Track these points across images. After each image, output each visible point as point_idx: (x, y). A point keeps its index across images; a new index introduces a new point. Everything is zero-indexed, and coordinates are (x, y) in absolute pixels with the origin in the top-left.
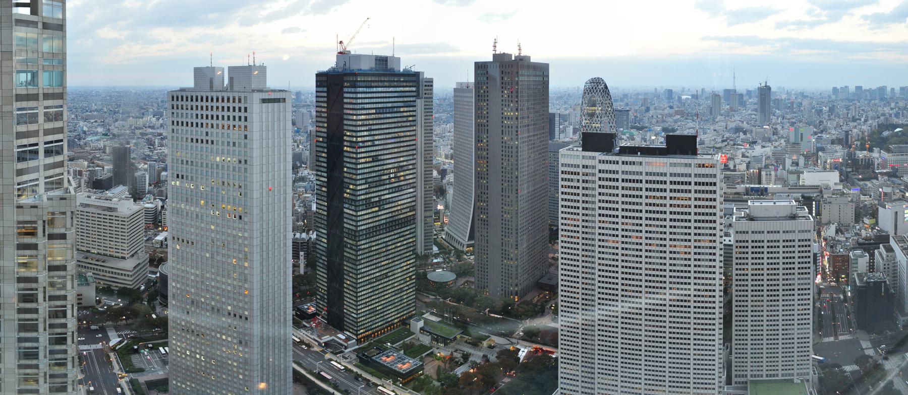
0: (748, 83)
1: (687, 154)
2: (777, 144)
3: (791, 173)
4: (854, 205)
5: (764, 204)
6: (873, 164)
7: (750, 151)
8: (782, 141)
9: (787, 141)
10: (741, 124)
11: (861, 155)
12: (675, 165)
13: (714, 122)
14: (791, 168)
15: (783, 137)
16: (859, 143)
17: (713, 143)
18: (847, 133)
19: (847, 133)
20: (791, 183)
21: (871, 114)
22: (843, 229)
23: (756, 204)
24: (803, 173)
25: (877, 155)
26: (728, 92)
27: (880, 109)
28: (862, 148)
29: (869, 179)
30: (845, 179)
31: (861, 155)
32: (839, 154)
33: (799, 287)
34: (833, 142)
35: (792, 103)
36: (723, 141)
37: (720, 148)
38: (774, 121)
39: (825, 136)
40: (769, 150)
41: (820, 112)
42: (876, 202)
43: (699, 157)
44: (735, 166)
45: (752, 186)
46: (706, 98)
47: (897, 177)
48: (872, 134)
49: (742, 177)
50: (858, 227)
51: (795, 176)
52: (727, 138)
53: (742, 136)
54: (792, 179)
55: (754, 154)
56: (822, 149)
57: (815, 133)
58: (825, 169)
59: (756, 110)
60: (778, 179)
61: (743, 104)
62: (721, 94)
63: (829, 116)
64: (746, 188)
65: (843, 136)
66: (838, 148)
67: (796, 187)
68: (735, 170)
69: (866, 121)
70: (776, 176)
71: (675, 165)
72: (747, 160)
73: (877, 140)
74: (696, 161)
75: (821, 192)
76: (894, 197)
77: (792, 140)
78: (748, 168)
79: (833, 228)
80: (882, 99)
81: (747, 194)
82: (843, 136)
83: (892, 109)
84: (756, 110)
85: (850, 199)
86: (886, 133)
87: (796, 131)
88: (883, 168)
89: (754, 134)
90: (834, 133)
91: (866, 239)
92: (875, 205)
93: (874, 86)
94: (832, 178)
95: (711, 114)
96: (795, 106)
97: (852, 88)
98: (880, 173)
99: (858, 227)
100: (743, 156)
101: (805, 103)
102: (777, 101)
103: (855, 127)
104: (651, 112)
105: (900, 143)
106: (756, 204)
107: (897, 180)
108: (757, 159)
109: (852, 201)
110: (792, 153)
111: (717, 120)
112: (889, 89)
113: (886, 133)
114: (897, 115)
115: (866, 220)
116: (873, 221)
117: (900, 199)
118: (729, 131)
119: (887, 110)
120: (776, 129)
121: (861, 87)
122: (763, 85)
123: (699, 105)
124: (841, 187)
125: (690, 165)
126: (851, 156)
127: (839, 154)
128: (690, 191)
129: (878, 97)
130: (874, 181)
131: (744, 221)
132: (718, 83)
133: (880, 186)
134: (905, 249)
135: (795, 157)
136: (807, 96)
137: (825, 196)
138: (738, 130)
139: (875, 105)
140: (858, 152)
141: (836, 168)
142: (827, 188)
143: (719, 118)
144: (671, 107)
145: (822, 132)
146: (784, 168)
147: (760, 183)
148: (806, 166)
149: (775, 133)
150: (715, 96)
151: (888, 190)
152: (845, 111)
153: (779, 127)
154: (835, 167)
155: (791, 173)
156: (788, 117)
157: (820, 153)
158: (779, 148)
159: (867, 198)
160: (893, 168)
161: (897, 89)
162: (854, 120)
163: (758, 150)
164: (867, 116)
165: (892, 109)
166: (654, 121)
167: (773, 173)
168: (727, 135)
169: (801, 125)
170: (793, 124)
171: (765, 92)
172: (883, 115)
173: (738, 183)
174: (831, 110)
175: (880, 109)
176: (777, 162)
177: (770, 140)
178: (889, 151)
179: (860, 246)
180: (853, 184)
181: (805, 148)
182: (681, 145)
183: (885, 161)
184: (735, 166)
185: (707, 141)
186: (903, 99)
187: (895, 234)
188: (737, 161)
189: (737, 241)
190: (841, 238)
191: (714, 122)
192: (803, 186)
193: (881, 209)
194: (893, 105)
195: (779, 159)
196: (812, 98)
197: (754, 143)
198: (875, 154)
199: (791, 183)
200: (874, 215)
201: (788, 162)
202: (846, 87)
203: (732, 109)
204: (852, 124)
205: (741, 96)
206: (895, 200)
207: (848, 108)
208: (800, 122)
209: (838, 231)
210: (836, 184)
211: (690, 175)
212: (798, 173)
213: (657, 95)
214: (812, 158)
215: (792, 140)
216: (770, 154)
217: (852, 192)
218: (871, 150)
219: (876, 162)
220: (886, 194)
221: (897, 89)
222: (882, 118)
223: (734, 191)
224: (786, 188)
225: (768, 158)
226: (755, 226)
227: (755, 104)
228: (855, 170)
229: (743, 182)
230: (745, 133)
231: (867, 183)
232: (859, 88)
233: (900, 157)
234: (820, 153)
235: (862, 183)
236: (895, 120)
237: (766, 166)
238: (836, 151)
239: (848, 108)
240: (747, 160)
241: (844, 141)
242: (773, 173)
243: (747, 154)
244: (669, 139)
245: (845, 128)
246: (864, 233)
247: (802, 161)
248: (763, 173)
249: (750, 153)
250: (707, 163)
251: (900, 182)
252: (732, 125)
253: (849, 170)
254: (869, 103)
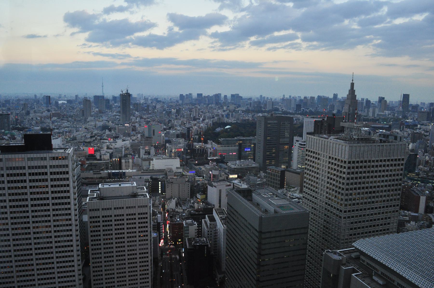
0: (112, 91)
1: (44, 150)
2: (135, 138)
3: (145, 160)
4: (190, 184)
5: (112, 186)
6: (206, 152)
7: (113, 144)
8: (139, 136)
9: (143, 136)
10: (107, 123)
11: (197, 145)
12: (32, 159)
13: (86, 121)
14: (144, 156)
15: (139, 133)
16: (197, 137)
17: (83, 138)
18: (189, 129)
19: (189, 129)
20: (145, 168)
21: (207, 114)
22: (181, 203)
23: (105, 186)
24: (152, 160)
25: (210, 146)
26: (97, 98)
27: (215, 111)
28: (200, 141)
29: (203, 164)
30: (185, 164)
31: (197, 145)
32: (181, 145)
33: (140, 252)
34: (178, 136)
35: (148, 106)
36: (91, 137)
37: (89, 142)
38: (133, 120)
39: (172, 131)
40: (128, 143)
41: (169, 113)
42: (206, 182)
43: (54, 151)
44: (101, 156)
45: (113, 171)
46: (80, 103)
47: (223, 162)
48: (208, 129)
49: (107, 164)
50: (192, 201)
51: (147, 163)
52: (96, 134)
53: (107, 132)
54: (145, 164)
55: (116, 146)
56: (169, 142)
57: (165, 129)
58: (170, 157)
59: (119, 112)
60: (135, 165)
61: (109, 107)
62: (92, 100)
63: (176, 116)
64: (109, 173)
65: (185, 132)
66: (182, 140)
67: (148, 171)
68: (100, 160)
69: (204, 120)
70: (133, 162)
71: (32, 159)
72: (111, 151)
73: (210, 135)
74: (50, 155)
75: (166, 174)
76: (221, 178)
77: (146, 134)
78: (111, 156)
79: (174, 202)
80: (217, 103)
81: (110, 178)
82: (185, 132)
83: (224, 111)
84: (119, 112)
85: (187, 179)
86: (218, 130)
87: (149, 127)
88: (214, 156)
89: (117, 131)
90: (179, 129)
91: (198, 210)
92: (206, 184)
93: (211, 93)
94: (175, 164)
95: (83, 115)
96: (150, 109)
97: (195, 96)
98: (211, 160)
99: (192, 201)
100: (108, 148)
101: (158, 106)
102: (137, 106)
103: (195, 125)
104: (32, 115)
105: (229, 137)
106: (105, 186)
107: (224, 165)
108: (118, 150)
109: (188, 181)
110: (146, 145)
111: (88, 120)
112: (223, 96)
113: (218, 130)
114: (228, 116)
115: (199, 196)
116: (204, 196)
117: (224, 180)
118: (97, 129)
119: (220, 112)
120: (134, 126)
121: (201, 95)
122: (124, 92)
123: (73, 108)
124: (181, 170)
125: (45, 159)
126: (190, 147)
127: (181, 145)
128: (47, 180)
129: (214, 102)
130: (207, 166)
131: (96, 201)
132: (90, 91)
133: (209, 169)
134: (223, 219)
135: (147, 148)
136: (160, 101)
137: (169, 178)
138: (105, 128)
139: (212, 108)
140: (195, 143)
141: (179, 156)
142: (171, 171)
143: (89, 118)
144: (48, 111)
145: (170, 128)
146: (139, 156)
147: (120, 169)
148: (156, 154)
149: (134, 129)
150: (86, 101)
151: (216, 173)
152: (189, 113)
153: (137, 125)
154: (179, 155)
155: (145, 160)
156: (145, 117)
157: (167, 145)
158: (136, 141)
159: (201, 178)
160: (221, 156)
161: (229, 96)
162: (195, 119)
163: (120, 143)
164: (204, 117)
165: (224, 111)
166: (34, 122)
167: (131, 161)
168: (95, 132)
169: (153, 123)
170: (148, 123)
171: (126, 98)
172: (217, 115)
173: (102, 170)
174: (178, 112)
175: (215, 111)
176: (134, 152)
177: (129, 135)
178: (218, 143)
179: (192, 216)
180: (191, 169)
181: (156, 141)
182: (39, 142)
183: (215, 150)
184: (101, 156)
185: (78, 137)
186: (233, 104)
187: (220, 206)
188: (103, 152)
189: (91, 218)
190: (180, 210)
191: (86, 121)
192: (153, 170)
193: (209, 187)
194: (225, 108)
195: (135, 149)
196: (164, 103)
197: (117, 137)
198: (209, 146)
199: (145, 168)
200: (204, 192)
201: (142, 152)
202: (190, 94)
203: (100, 112)
204: (193, 122)
205: (108, 101)
206: (220, 181)
207: (191, 110)
208: (154, 121)
209: (178, 204)
210: (177, 168)
211: (46, 167)
212: (150, 160)
213: (37, 101)
214: (161, 149)
215: (146, 134)
216: (129, 146)
217: (189, 174)
218: (206, 142)
219: (209, 151)
220: (214, 176)
221: (229, 96)
222: (216, 118)
223: (99, 176)
224: (140, 172)
225: (127, 149)
226: (106, 204)
227: (119, 107)
228: (193, 157)
229: (107, 169)
230: (110, 130)
231: (201, 167)
232: (199, 95)
233: (227, 148)
234: (167, 145)
235: (198, 167)
236: (226, 120)
237: (126, 156)
238: (180, 143)
239: (191, 110)
240: (111, 151)
241: (186, 135)
242: (131, 161)
243: (111, 147)
244: (26, 137)
245: (187, 125)
246: (196, 205)
247: (153, 151)
248: (123, 161)
249: (114, 145)
250: (60, 156)
251: (226, 167)
252: (100, 124)
253: (188, 157)
254: (207, 107)
